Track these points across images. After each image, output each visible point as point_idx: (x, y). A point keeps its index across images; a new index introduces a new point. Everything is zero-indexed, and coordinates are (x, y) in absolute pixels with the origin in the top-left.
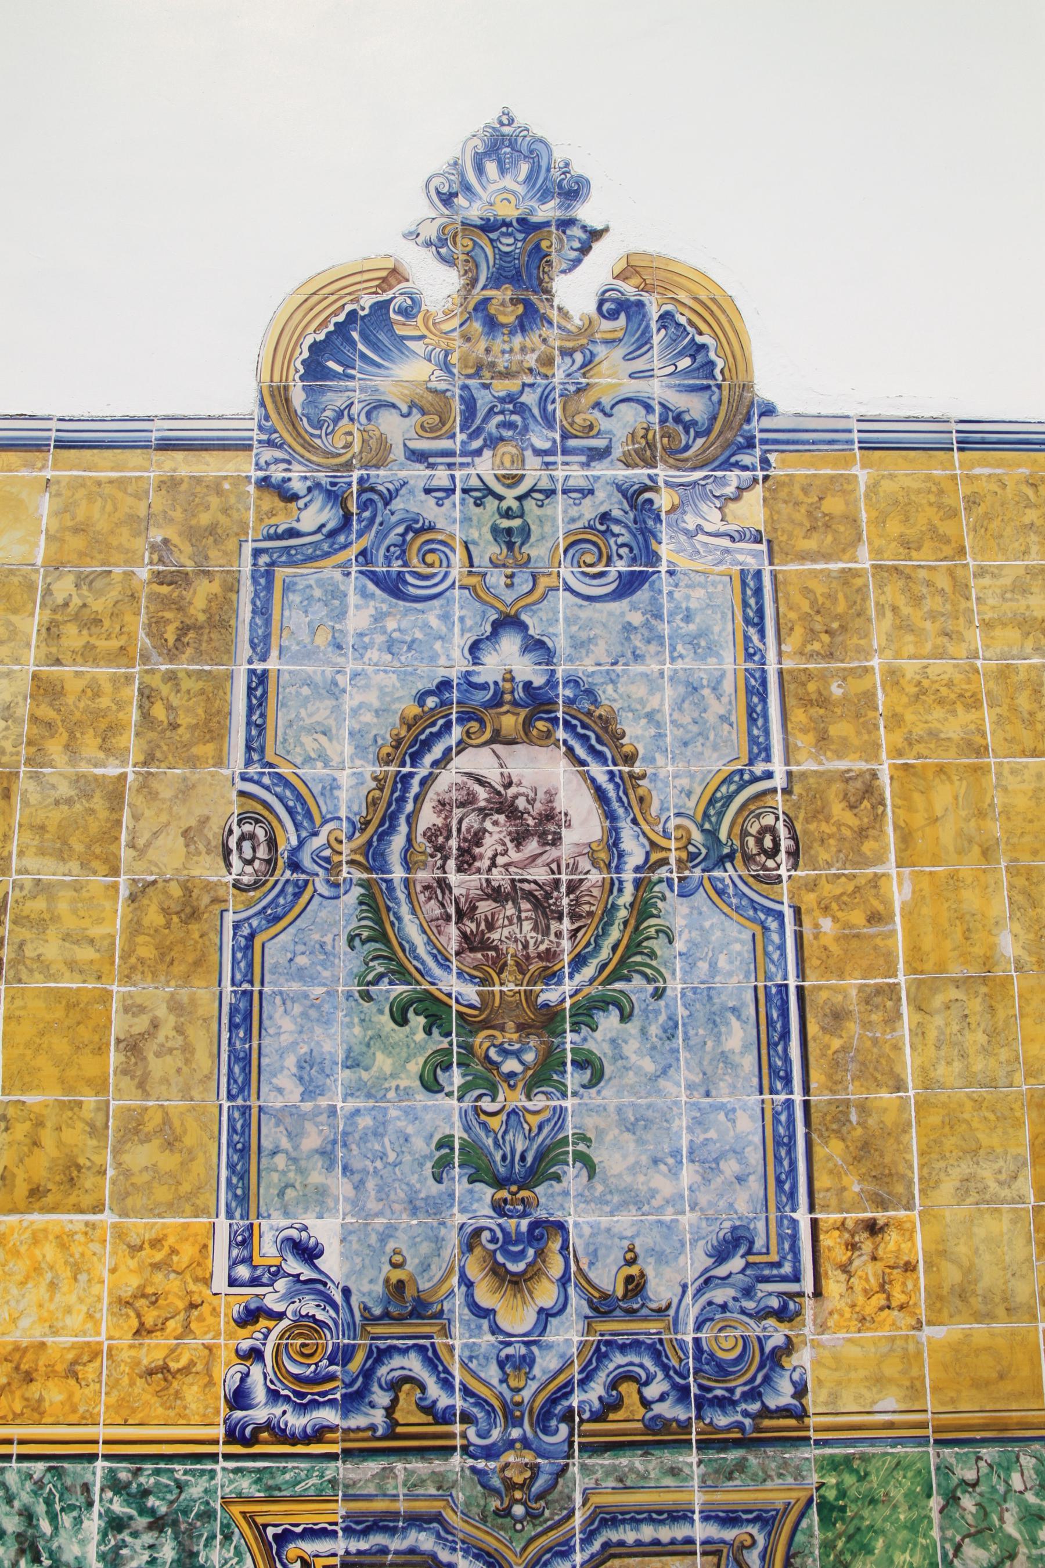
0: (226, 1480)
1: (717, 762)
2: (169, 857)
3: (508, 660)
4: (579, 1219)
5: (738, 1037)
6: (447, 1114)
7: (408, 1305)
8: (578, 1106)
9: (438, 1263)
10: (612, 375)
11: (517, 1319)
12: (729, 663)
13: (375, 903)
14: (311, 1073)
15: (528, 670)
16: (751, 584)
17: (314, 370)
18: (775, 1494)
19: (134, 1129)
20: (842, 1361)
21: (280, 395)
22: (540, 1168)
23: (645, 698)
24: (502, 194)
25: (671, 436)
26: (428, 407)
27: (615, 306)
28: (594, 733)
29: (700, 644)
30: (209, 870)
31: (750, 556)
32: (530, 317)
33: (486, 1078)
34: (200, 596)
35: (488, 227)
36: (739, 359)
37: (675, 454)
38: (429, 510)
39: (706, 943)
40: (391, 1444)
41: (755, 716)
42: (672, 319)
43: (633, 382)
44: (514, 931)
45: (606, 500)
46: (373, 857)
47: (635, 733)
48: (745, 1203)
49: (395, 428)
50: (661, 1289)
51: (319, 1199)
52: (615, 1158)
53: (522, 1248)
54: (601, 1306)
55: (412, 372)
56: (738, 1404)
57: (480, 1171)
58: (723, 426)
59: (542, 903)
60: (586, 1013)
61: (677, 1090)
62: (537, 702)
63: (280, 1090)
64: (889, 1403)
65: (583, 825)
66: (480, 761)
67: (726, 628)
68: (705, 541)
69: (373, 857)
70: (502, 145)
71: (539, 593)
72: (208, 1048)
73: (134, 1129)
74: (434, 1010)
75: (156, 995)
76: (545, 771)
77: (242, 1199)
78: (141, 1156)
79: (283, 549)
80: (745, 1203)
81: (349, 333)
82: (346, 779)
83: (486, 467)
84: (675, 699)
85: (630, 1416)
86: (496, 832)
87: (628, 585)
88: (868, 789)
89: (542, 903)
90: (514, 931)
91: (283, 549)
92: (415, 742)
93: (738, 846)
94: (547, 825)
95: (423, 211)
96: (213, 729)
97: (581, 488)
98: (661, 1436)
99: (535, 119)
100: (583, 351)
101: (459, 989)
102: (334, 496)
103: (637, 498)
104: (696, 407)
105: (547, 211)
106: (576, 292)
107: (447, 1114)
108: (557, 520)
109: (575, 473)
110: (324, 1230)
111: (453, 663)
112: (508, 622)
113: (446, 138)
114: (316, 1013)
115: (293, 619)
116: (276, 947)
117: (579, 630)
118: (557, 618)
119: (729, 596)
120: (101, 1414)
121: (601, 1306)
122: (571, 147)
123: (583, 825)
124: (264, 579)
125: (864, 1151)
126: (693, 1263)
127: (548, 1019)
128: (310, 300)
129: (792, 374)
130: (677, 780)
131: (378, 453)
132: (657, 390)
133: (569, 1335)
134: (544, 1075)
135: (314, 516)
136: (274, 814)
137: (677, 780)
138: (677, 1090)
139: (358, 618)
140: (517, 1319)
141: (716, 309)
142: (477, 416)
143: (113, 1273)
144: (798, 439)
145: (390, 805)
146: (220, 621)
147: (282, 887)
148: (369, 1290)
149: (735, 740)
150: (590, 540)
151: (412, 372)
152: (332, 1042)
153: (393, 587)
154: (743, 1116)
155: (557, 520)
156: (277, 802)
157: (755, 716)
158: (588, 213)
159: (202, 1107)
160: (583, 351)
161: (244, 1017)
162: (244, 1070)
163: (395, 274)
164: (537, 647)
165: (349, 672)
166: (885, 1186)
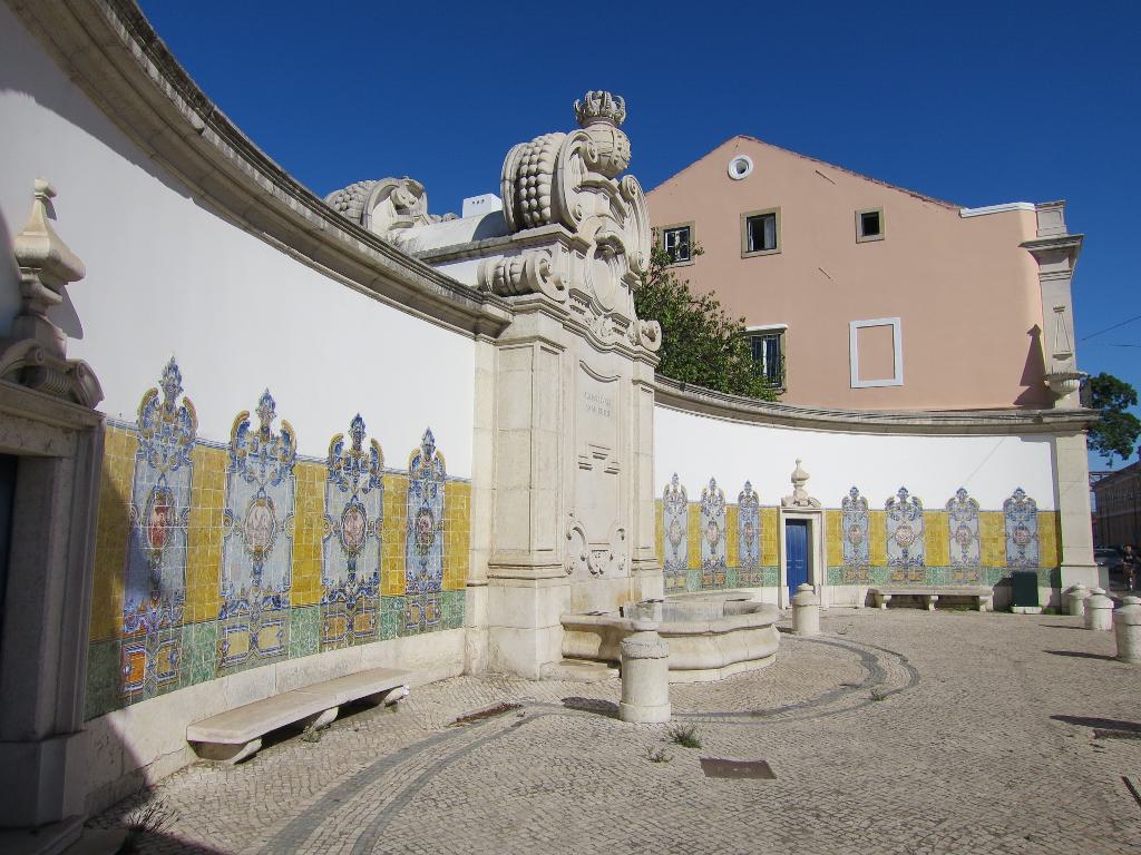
7: (417, 579)
20: (444, 586)
24: (428, 441)
42: (440, 461)
56: (436, 588)
58: (442, 477)
76: (427, 519)
82: (414, 519)
106: (433, 456)
108: (430, 487)
122: (434, 436)
129: (449, 472)
135: (412, 485)
137: (437, 520)
142: (426, 473)
151: (420, 466)
155: (430, 487)
165: (414, 504)
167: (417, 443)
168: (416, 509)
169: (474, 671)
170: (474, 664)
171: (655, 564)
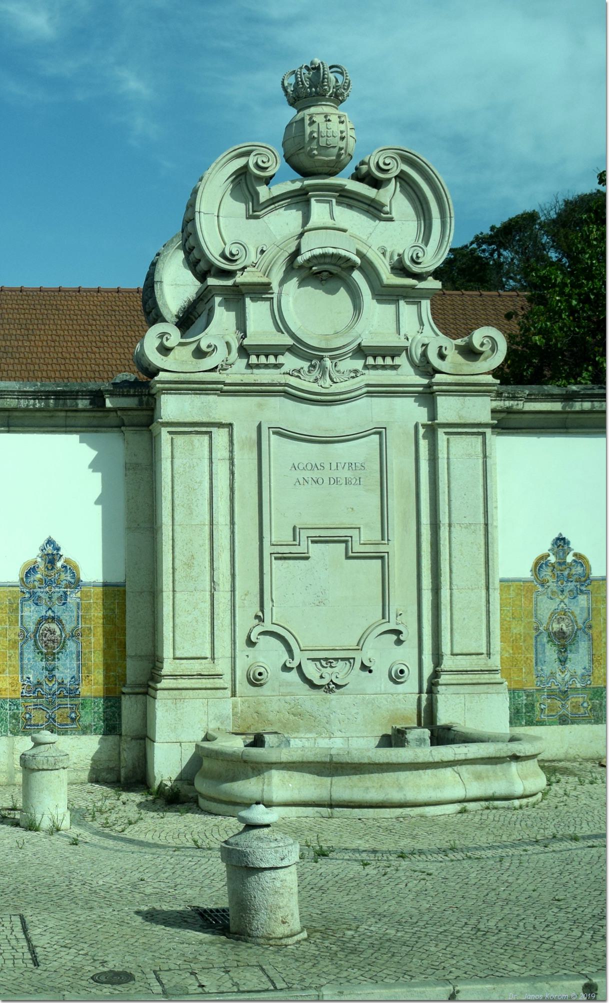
0: (21, 701)
1: (73, 626)
2: (13, 636)
3: (50, 613)
4: (57, 675)
5: (74, 656)
6: (43, 664)
7: (39, 684)
8: (57, 663)
9: (42, 679)
10: (63, 576)
11: (51, 685)
12: (75, 614)
13: (35, 641)
14: (29, 659)
15: (52, 614)
16: (78, 604)
17: (26, 576)
18: (77, 702)
19: (10, 666)
21: (22, 579)
22: (53, 669)
23: (65, 617)
24: (50, 549)
25: (69, 585)
26: (40, 580)
27: (64, 567)
28: (59, 621)
29: (72, 611)
30: (17, 638)
31: (78, 600)
32: (53, 568)
33: (47, 660)
34: (15, 605)
35: (48, 554)
36: (79, 574)
37: (70, 588)
38: (41, 595)
39: (71, 646)
40: (37, 697)
41: (78, 620)
43: (67, 577)
44: (50, 644)
45: (61, 593)
46: (35, 636)
47: (64, 622)
48: (74, 673)
49: (36, 584)
50: (65, 682)
51: (30, 673)
52: (61, 669)
53: (51, 678)
54: (59, 684)
55: (39, 576)
56: (73, 694)
57: (47, 669)
59: (54, 642)
60: (58, 653)
61: (67, 662)
62: (53, 618)
63: (26, 661)
64: (89, 694)
65: (58, 633)
66: (46, 625)
67: (75, 610)
68: (74, 597)
69: (35, 636)
70: (50, 542)
71: (53, 605)
72: (18, 657)
73: (10, 666)
74: (42, 653)
75: (12, 651)
76: (53, 626)
77: (22, 673)
78: (11, 669)
79: (24, 600)
80: (74, 673)
81: (31, 571)
82: (32, 627)
83: (47, 589)
84: (69, 618)
85: (62, 695)
86: (49, 633)
87: (64, 604)
88: (90, 628)
89: (54, 642)
90: (50, 644)
91: (24, 600)
92: (39, 623)
93: (75, 635)
94: (53, 633)
95: (39, 552)
96: (17, 622)
97: (58, 591)
98: (65, 697)
99: (54, 538)
100: (59, 572)
101: (44, 651)
102: (29, 593)
103: (65, 593)
104: (73, 581)
105: (55, 552)
106: (59, 564)
107: (43, 664)
108: (55, 596)
109: (57, 589)
110: (31, 676)
111: (43, 613)
112: (50, 608)
113: (42, 541)
114: (29, 653)
115: (25, 609)
116: (25, 646)
117: (58, 610)
118: (55, 608)
119: (75, 605)
120: (8, 695)
121: (59, 684)
122: (59, 542)
123: (58, 633)
124: (22, 603)
125: (87, 668)
126: (69, 679)
127: (54, 654)
128: (26, 565)
130: (69, 627)
131: (34, 587)
132: (69, 578)
133: (56, 686)
134: (54, 660)
135: (27, 595)
136: (24, 630)
137: (69, 627)
138: (67, 662)
139: (33, 608)
140: (51, 685)
141: (76, 567)
142: (47, 582)
143: (8, 680)
144: (85, 585)
145: (37, 630)
146: (17, 609)
147: (25, 639)
148: (35, 682)
149: (75, 622)
150: (60, 598)
151: (39, 576)
152: (31, 656)
153: (37, 604)
154: (75, 664)
155: (55, 596)
156: (24, 630)
157: (78, 620)
158: (61, 553)
159: (16, 661)
160: (59, 572)
161: (22, 654)
162: (22, 659)
163: (36, 562)
164: (53, 612)
165: (31, 614)
166: (89, 672)
167: (32, 553)
168: (35, 617)
169: (122, 779)
170: (123, 772)
171: (498, 677)
